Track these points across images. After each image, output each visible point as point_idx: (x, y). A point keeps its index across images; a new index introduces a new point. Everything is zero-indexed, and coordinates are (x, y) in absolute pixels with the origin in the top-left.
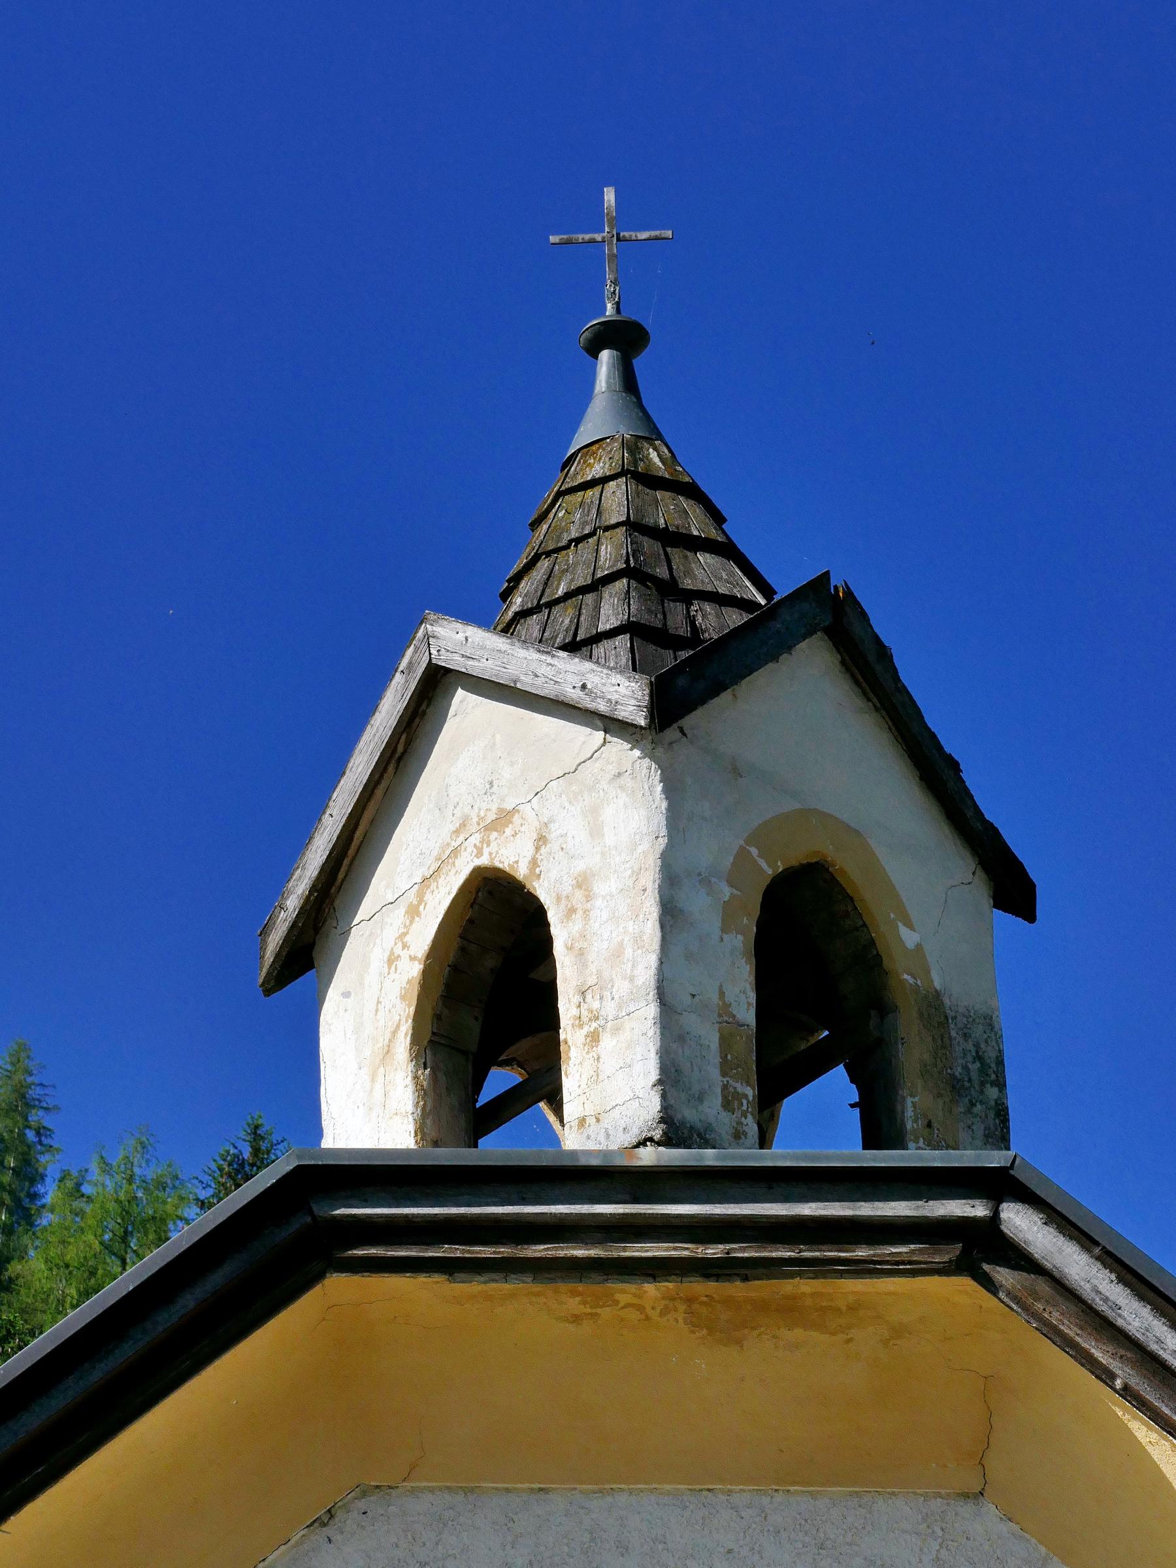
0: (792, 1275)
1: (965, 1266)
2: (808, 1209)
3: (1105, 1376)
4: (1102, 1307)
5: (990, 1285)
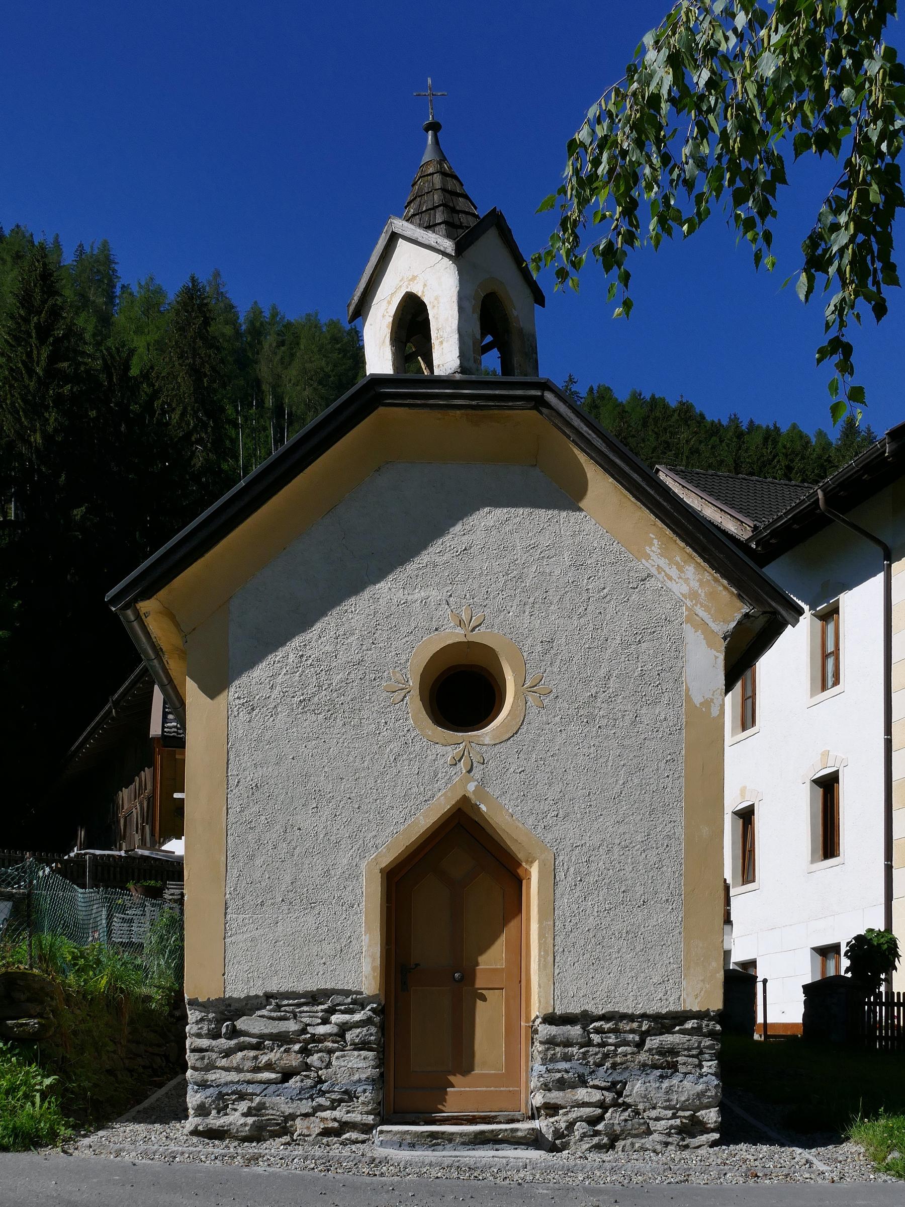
0: (493, 409)
1: (535, 408)
2: (497, 392)
3: (568, 437)
4: (568, 419)
5: (541, 413)
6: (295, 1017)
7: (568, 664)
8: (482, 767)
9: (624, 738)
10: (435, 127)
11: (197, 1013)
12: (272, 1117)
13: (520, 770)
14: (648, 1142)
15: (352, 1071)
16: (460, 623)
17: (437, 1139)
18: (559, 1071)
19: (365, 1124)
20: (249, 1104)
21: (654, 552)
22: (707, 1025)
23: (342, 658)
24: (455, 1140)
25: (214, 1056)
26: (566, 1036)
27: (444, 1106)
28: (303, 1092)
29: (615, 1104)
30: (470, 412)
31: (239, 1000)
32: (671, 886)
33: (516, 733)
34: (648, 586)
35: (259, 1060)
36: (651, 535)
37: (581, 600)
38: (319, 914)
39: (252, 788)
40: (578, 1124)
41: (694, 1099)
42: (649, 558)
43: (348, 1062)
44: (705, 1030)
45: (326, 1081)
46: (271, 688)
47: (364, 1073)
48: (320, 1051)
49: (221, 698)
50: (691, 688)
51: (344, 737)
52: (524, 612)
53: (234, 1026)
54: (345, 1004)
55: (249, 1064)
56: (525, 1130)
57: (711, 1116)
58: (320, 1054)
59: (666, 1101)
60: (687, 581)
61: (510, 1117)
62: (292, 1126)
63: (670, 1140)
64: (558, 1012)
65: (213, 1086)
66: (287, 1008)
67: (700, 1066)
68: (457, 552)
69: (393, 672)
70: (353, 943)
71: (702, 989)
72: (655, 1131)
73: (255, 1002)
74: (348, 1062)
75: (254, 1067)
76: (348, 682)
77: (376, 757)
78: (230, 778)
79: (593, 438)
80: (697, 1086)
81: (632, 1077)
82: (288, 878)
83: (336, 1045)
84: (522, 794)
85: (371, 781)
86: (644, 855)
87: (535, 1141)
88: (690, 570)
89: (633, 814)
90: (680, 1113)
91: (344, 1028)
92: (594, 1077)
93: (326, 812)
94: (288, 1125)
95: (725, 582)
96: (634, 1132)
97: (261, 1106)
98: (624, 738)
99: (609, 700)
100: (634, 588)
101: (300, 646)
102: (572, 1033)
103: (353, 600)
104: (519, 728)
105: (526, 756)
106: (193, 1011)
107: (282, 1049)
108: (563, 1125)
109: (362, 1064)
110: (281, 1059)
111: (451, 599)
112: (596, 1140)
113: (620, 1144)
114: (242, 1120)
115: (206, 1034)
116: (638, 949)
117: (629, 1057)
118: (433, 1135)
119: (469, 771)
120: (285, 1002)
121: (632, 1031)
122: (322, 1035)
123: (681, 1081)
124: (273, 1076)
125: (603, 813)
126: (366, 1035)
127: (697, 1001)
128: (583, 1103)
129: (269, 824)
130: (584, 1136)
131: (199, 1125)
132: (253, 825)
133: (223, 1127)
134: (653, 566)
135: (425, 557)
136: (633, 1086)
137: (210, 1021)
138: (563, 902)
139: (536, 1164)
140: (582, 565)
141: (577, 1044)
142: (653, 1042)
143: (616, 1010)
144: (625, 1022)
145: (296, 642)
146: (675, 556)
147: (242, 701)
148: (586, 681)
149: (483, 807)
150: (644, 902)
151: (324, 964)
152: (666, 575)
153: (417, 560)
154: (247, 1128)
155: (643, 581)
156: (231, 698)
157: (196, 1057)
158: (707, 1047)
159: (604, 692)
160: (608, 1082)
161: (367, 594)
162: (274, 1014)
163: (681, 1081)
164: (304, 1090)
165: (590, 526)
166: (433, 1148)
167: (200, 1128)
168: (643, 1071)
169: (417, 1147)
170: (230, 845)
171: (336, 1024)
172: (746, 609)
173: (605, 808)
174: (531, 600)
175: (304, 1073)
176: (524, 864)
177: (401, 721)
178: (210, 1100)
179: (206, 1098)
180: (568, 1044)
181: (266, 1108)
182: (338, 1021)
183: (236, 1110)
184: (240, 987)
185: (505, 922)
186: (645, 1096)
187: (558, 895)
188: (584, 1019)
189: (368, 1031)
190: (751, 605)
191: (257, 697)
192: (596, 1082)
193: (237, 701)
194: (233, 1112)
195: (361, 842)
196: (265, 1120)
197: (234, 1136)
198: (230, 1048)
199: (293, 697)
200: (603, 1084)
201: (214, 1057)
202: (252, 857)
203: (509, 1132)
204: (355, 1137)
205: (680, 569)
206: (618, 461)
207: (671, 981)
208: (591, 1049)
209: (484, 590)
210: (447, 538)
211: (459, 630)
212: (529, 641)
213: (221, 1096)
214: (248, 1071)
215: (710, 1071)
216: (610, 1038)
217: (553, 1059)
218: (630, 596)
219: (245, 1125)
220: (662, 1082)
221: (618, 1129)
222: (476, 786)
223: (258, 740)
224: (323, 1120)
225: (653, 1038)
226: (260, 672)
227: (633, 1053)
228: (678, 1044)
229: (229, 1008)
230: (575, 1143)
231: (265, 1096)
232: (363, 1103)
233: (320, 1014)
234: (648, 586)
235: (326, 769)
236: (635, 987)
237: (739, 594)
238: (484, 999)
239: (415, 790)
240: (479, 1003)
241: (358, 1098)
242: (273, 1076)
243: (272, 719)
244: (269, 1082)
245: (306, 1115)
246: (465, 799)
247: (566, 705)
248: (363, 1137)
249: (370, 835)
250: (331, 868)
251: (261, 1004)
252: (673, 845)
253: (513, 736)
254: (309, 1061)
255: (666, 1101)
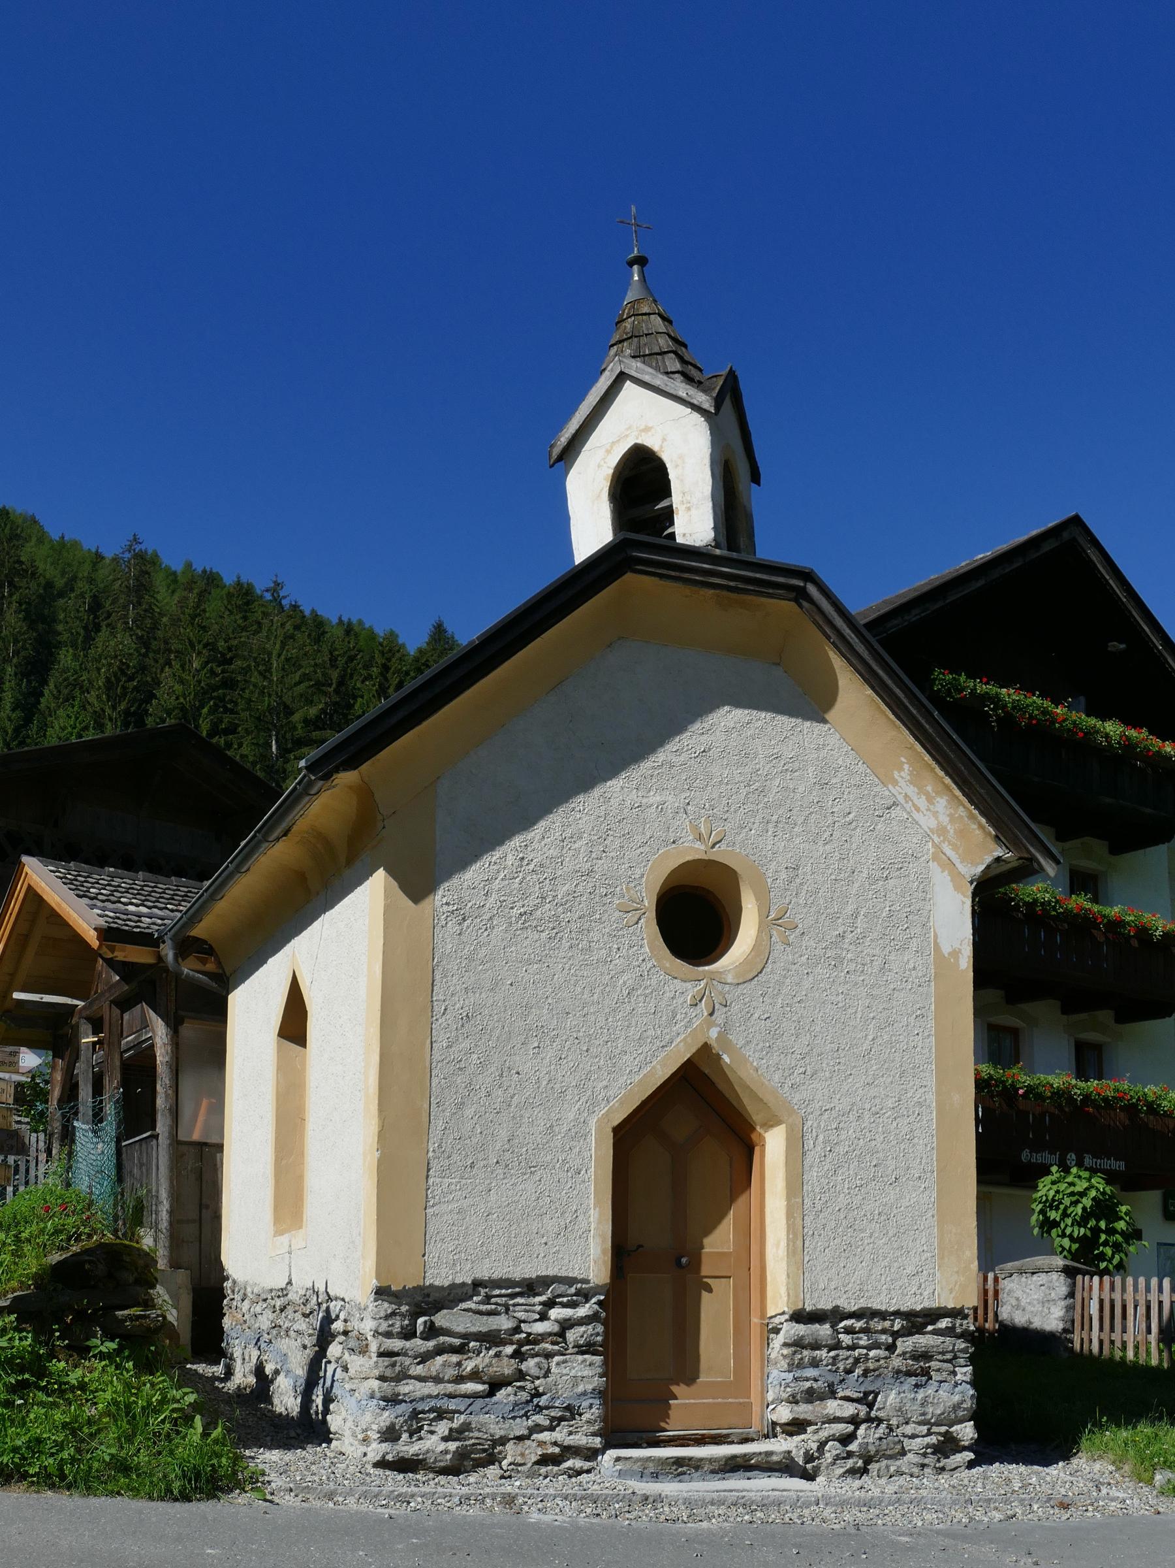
0: (750, 594)
1: (796, 600)
2: (758, 576)
3: (828, 637)
4: (831, 618)
5: (800, 606)
6: (507, 1311)
7: (814, 896)
8: (725, 1009)
9: (873, 987)
10: (641, 261)
11: (386, 1305)
12: (477, 1441)
13: (766, 1016)
14: (903, 1463)
15: (576, 1380)
16: (700, 838)
17: (682, 1466)
18: (807, 1379)
19: (589, 1449)
20: (450, 1425)
21: (902, 778)
22: (961, 1325)
23: (569, 866)
24: (703, 1468)
25: (408, 1361)
26: (814, 1337)
27: (667, 1423)
28: (516, 1408)
29: (869, 1420)
30: (725, 593)
31: (441, 1289)
32: (923, 1162)
33: (761, 972)
34: (893, 816)
35: (463, 1367)
36: (903, 759)
37: (827, 824)
38: (540, 1181)
39: (462, 1018)
40: (830, 1443)
41: (950, 1412)
42: (897, 785)
43: (570, 1370)
44: (958, 1330)
45: (544, 1394)
46: (486, 895)
47: (590, 1383)
48: (537, 1355)
49: (426, 904)
50: (939, 934)
51: (571, 962)
52: (767, 832)
53: (432, 1323)
54: (567, 1296)
55: (451, 1373)
56: (781, 1453)
57: (967, 1432)
58: (537, 1360)
59: (922, 1414)
60: (935, 814)
61: (744, 1436)
62: (500, 1453)
63: (926, 1461)
64: (808, 1308)
65: (405, 1402)
66: (498, 1300)
67: (954, 1373)
68: (695, 753)
69: (626, 888)
70: (580, 1218)
71: (956, 1283)
72: (910, 1451)
73: (459, 1291)
74: (570, 1370)
75: (457, 1376)
76: (576, 895)
77: (607, 989)
78: (435, 1003)
79: (855, 643)
80: (953, 1396)
81: (886, 1386)
82: (504, 1134)
83: (556, 1347)
84: (768, 1045)
85: (602, 1019)
86: (895, 1124)
87: (786, 1467)
88: (942, 803)
89: (883, 1076)
90: (935, 1429)
91: (566, 1325)
92: (844, 1387)
93: (549, 1054)
94: (495, 1451)
95: (983, 821)
96: (888, 1452)
97: (466, 1427)
98: (873, 987)
99: (857, 942)
100: (880, 817)
101: (520, 846)
102: (822, 1333)
103: (581, 798)
104: (764, 967)
105: (771, 1001)
106: (380, 1302)
107: (492, 1352)
108: (815, 1446)
109: (587, 1372)
110: (490, 1365)
111: (689, 807)
112: (850, 1463)
113: (873, 1467)
114: (442, 1446)
115: (398, 1333)
116: (891, 1234)
117: (882, 1362)
118: (679, 1462)
119: (711, 1014)
120: (497, 1292)
121: (884, 1331)
122: (539, 1335)
123: (937, 1391)
124: (480, 1387)
125: (853, 1072)
126: (592, 1335)
127: (952, 1296)
128: (834, 1418)
129: (482, 1065)
130: (837, 1458)
131: (387, 1453)
132: (462, 1065)
133: (417, 1455)
134: (900, 793)
135: (661, 756)
136: (886, 1397)
137: (403, 1316)
138: (812, 1176)
139: (830, 1498)
140: (827, 784)
141: (825, 1346)
142: (905, 1344)
143: (870, 1305)
144: (876, 1320)
145: (516, 841)
146: (926, 786)
147: (451, 908)
148: (834, 918)
149: (726, 1058)
150: (896, 1178)
151: (546, 1244)
152: (914, 805)
153: (652, 758)
154: (449, 1457)
155: (888, 808)
156: (438, 903)
157: (386, 1364)
158: (961, 1351)
159: (852, 932)
160: (860, 1392)
161: (597, 792)
162: (483, 1308)
163: (937, 1391)
164: (518, 1405)
165: (834, 740)
166: (678, 1478)
167: (389, 1457)
168: (897, 1379)
169: (660, 1477)
170: (434, 1089)
171: (556, 1321)
172: (999, 852)
173: (855, 1067)
174: (775, 818)
175: (518, 1384)
176: (758, 1128)
177: (636, 948)
178: (402, 1419)
179: (396, 1418)
180: (816, 1346)
181: (470, 1430)
182: (560, 1317)
183: (432, 1432)
184: (444, 1272)
185: (733, 1199)
186: (900, 1410)
187: (806, 1168)
188: (835, 1316)
189: (594, 1329)
190: (1007, 848)
191: (470, 905)
192: (848, 1393)
193: (445, 908)
194: (429, 1435)
195: (589, 1093)
196: (470, 1445)
197: (430, 1467)
198: (428, 1351)
199: (512, 908)
200: (855, 1395)
201: (407, 1363)
202: (461, 1105)
203: (763, 1456)
204: (580, 1465)
205: (930, 800)
206: (881, 672)
207: (924, 1272)
208: (841, 1352)
209: (724, 802)
210: (685, 735)
211: (698, 845)
212: (773, 866)
213: (415, 1414)
214: (449, 1382)
215: (964, 1378)
216: (861, 1339)
217: (800, 1365)
218: (876, 825)
219: (446, 1452)
220: (916, 1392)
221: (872, 1449)
222: (719, 1033)
223: (470, 959)
224: (541, 1444)
225: (905, 1339)
226: (473, 874)
227: (886, 1358)
228: (933, 1347)
229: (427, 1299)
230: (827, 1468)
231: (471, 1414)
232: (588, 1422)
233: (538, 1308)
234: (893, 816)
235: (550, 1000)
236: (888, 1279)
237: (997, 836)
238: (710, 1290)
239: (651, 1033)
240: (705, 1294)
241: (580, 1415)
242: (480, 1387)
243: (486, 933)
244: (475, 1396)
245: (520, 1438)
246: (706, 1048)
247: (812, 943)
248: (587, 1465)
249: (601, 1085)
250: (554, 1124)
251: (466, 1294)
252: (924, 1114)
253: (757, 975)
254: (523, 1367)
255: (922, 1414)
